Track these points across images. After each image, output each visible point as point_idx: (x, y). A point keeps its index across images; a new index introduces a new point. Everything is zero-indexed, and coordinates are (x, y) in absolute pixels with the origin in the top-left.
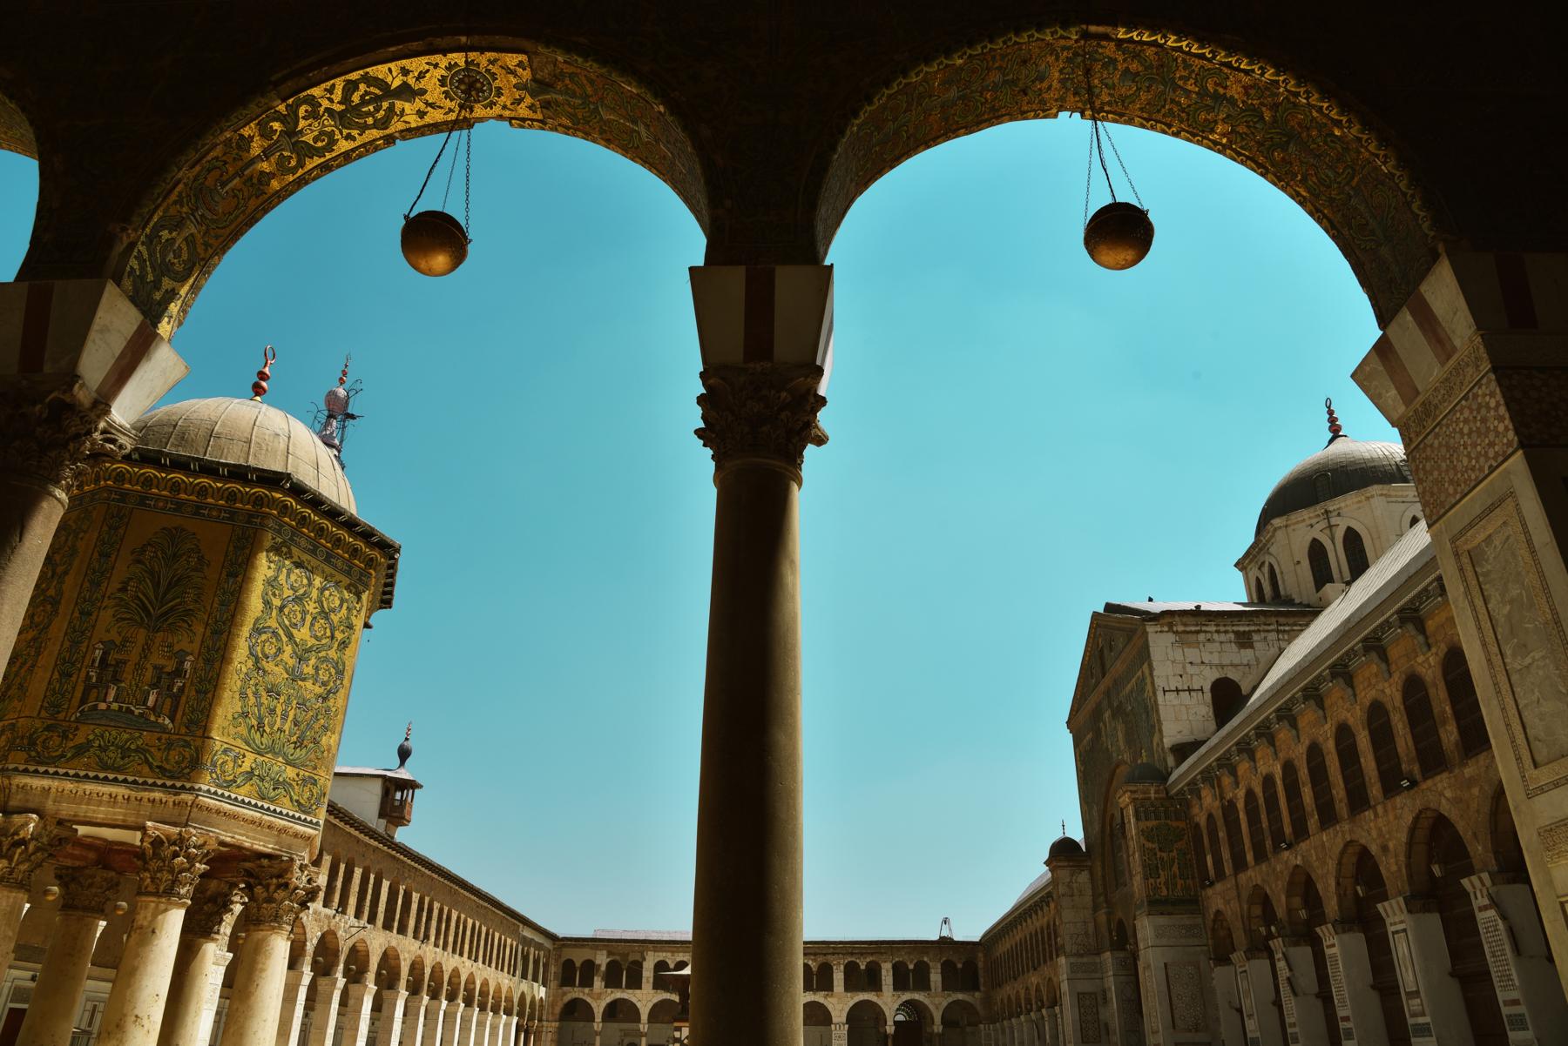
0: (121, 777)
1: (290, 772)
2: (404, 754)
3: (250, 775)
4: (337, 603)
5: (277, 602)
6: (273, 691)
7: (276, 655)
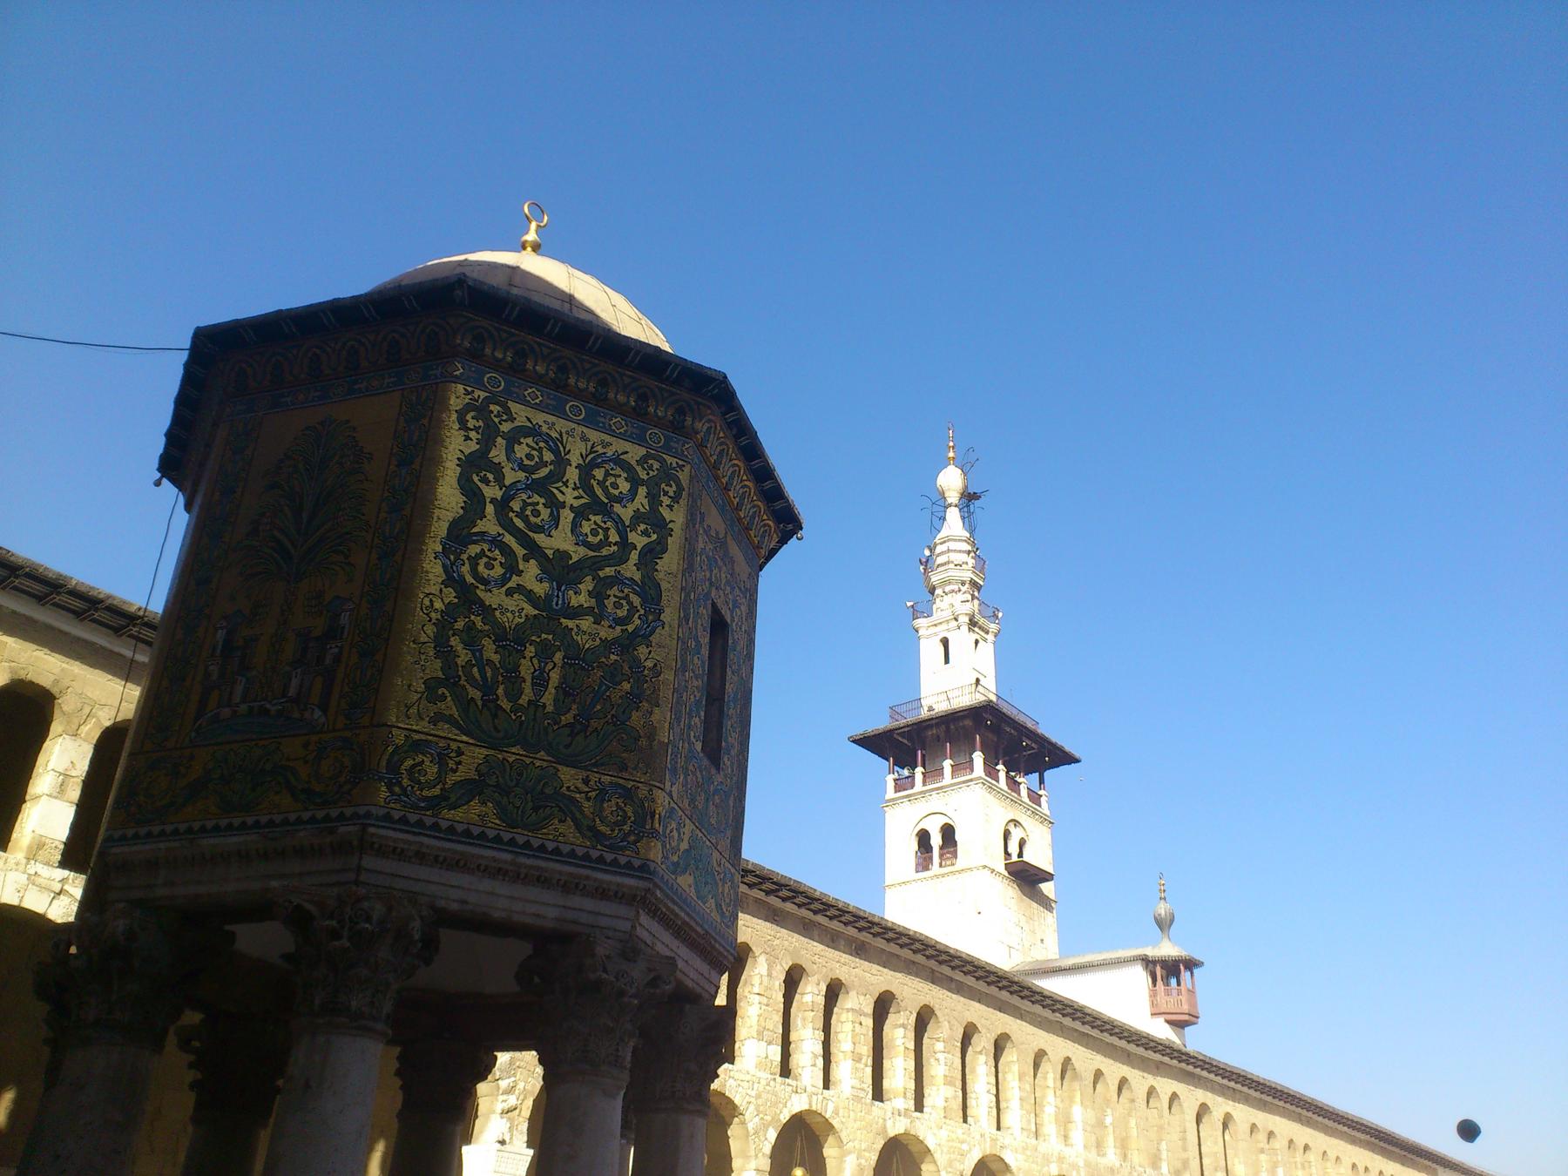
0: (250, 821)
1: (569, 777)
3: (473, 788)
4: (624, 486)
5: (492, 492)
6: (512, 641)
7: (504, 580)
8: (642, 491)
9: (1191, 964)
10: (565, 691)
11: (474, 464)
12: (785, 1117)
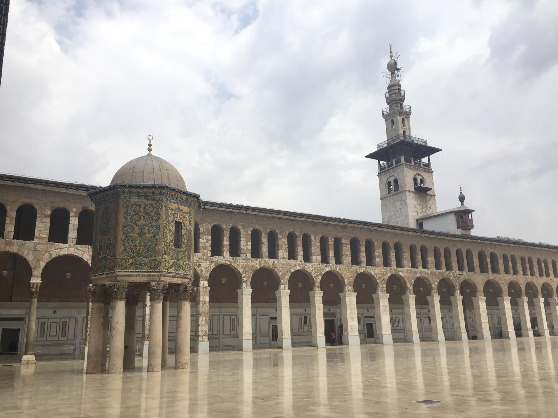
1: (146, 260)
2: (462, 199)
3: (132, 264)
4: (152, 209)
7: (133, 231)
8: (155, 210)
9: (470, 212)
10: (144, 246)
11: (126, 213)
12: (323, 273)
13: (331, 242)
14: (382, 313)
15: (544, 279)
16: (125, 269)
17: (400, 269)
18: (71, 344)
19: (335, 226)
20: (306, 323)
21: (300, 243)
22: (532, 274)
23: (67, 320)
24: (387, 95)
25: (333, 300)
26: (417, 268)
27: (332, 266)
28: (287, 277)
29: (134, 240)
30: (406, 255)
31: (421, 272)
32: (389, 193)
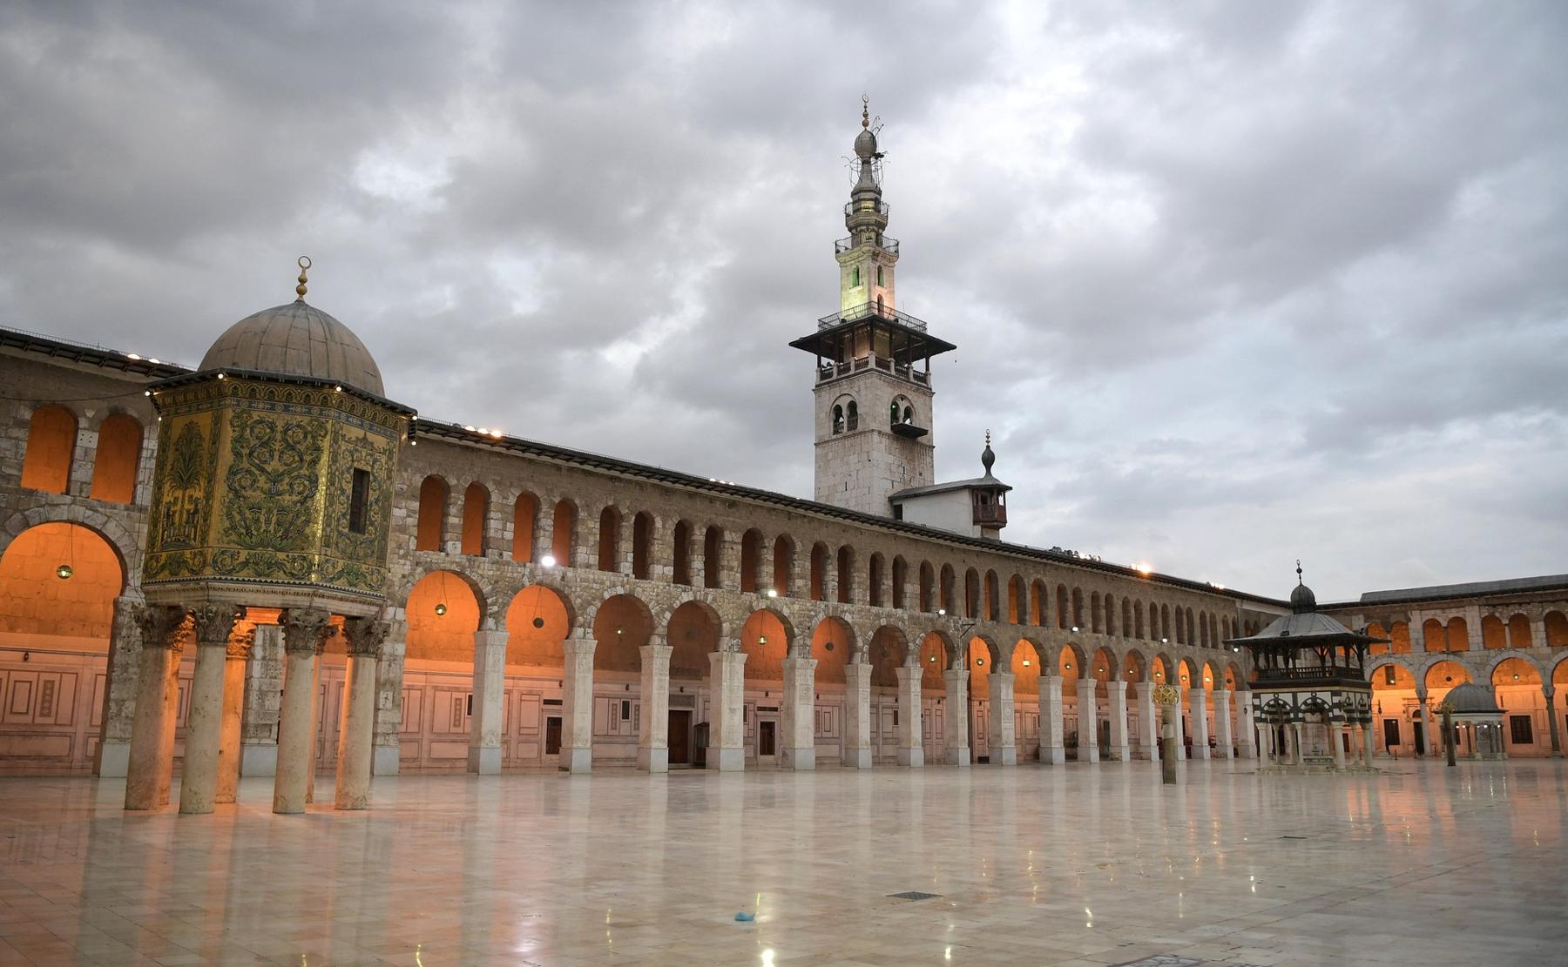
1: (281, 556)
3: (246, 564)
9: (1003, 489)
10: (279, 524)
12: (677, 605)
13: (699, 535)
14: (797, 702)
15: (1132, 643)
16: (230, 572)
17: (846, 607)
18: (63, 735)
19: (712, 500)
20: (626, 715)
21: (627, 531)
22: (1110, 632)
23: (56, 677)
24: (850, 210)
25: (691, 665)
26: (881, 605)
27: (697, 591)
28: (592, 611)
29: (254, 508)
30: (861, 577)
31: (889, 616)
32: (836, 432)
